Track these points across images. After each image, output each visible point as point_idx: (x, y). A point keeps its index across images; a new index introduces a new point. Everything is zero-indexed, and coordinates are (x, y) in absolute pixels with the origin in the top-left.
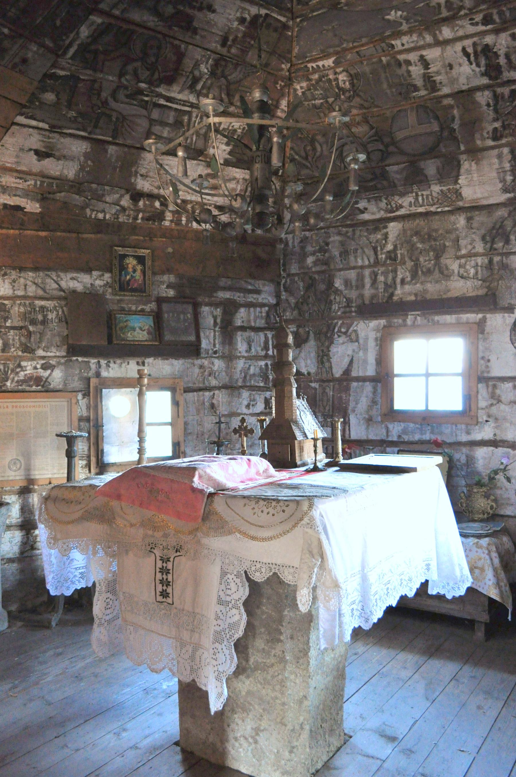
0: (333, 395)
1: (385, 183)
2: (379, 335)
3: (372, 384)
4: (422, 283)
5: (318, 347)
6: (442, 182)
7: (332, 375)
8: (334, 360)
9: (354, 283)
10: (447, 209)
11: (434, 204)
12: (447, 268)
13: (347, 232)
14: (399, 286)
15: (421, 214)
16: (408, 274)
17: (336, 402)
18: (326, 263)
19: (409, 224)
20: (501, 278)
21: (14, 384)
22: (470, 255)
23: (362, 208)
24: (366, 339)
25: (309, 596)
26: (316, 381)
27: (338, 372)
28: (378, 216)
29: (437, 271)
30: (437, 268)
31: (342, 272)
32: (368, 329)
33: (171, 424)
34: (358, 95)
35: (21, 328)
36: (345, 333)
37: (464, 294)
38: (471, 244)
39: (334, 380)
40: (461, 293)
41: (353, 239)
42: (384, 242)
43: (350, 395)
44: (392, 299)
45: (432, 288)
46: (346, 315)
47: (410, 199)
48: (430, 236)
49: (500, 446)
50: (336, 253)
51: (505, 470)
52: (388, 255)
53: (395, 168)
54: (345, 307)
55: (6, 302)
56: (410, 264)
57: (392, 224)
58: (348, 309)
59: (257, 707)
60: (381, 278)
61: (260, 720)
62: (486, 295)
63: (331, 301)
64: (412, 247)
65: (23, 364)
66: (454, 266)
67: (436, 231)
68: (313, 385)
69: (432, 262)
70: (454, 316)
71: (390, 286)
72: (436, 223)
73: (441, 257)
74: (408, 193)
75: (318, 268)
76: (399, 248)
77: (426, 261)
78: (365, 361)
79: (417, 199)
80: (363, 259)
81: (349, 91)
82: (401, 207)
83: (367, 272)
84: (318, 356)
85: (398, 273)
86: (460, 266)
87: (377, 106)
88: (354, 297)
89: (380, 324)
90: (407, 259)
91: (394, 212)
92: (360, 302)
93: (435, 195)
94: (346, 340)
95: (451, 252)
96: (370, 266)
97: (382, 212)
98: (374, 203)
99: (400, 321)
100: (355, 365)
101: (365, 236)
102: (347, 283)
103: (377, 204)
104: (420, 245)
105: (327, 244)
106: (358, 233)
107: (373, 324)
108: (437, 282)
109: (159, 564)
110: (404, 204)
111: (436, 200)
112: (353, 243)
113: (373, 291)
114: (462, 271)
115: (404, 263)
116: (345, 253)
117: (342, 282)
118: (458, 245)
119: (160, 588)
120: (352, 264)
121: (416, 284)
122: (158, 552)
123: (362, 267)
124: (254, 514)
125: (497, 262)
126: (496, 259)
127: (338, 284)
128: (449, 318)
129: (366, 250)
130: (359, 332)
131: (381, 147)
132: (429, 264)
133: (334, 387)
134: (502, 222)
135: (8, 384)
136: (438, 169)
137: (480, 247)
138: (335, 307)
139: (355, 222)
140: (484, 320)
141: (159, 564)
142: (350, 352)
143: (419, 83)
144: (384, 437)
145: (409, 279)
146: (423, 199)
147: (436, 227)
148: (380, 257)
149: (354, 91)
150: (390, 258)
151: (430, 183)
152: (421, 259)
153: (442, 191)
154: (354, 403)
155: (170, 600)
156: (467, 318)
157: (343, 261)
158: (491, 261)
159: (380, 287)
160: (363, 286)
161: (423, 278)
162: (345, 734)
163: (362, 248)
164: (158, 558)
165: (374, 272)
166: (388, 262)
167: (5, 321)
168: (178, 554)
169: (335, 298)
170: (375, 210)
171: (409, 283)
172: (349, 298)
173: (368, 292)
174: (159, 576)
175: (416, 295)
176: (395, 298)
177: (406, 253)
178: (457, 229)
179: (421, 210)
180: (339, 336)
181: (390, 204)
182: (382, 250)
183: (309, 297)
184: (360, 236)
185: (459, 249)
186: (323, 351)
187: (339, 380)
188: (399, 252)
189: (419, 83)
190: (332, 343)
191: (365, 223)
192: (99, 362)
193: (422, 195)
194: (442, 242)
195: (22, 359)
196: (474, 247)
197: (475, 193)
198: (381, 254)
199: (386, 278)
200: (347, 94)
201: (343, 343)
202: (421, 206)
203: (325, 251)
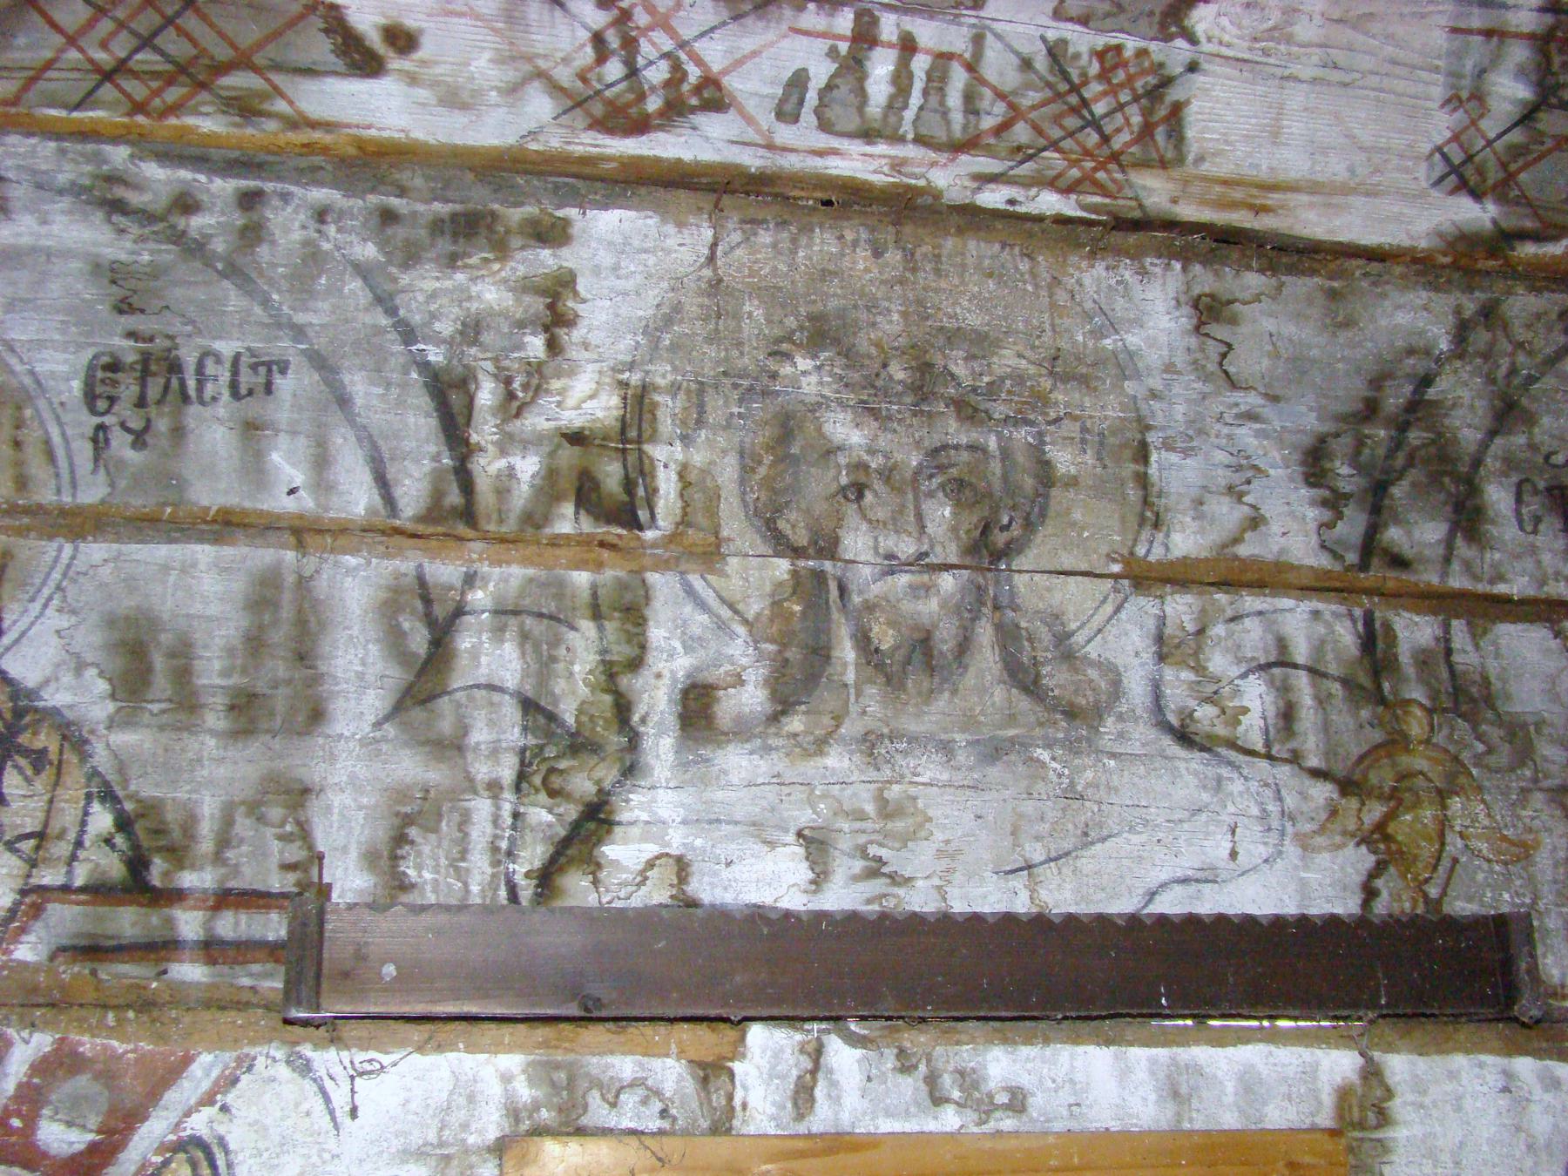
12: (1068, 655)
16: (739, 650)
28: (491, 131)
29: (987, 657)
30: (985, 633)
42: (536, 345)
52: (569, 456)
56: (753, 574)
60: (490, 658)
66: (1122, 638)
69: (947, 582)
71: (580, 745)
76: (666, 425)
77: (891, 565)
79: (853, 66)
85: (657, 634)
90: (734, 525)
96: (384, 531)
97: (540, 106)
101: (362, 270)
110: (734, 83)
114: (1178, 685)
129: (359, 385)
132: (916, 591)
148: (487, 467)
150: (586, 494)
152: (857, 543)
159: (480, 735)
161: (871, 706)
165: (424, 591)
166: (567, 520)
177: (727, 473)
182: (512, 406)
188: (665, 456)
191: (371, 163)
193: (908, 46)
199: (544, 662)
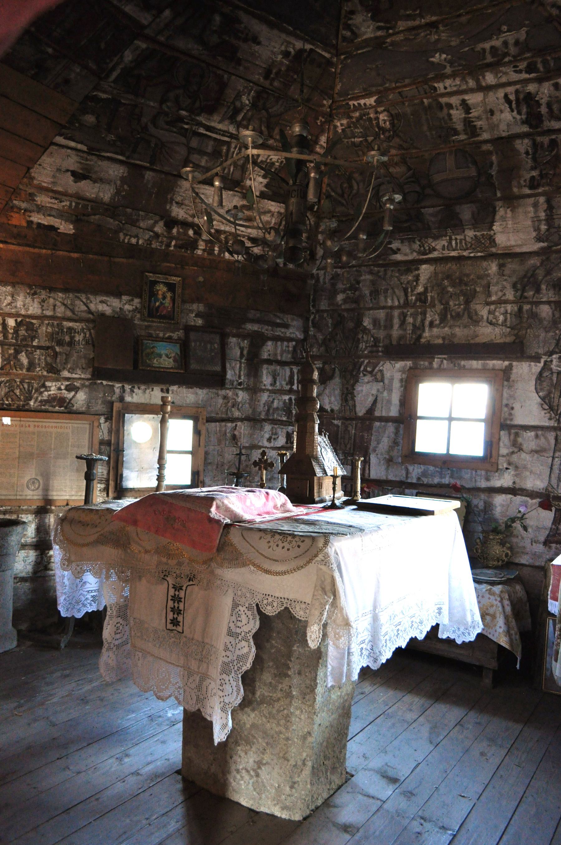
0: (355, 433)
1: (419, 224)
2: (404, 376)
3: (394, 425)
4: (450, 327)
5: (343, 385)
6: (476, 228)
7: (356, 414)
8: (358, 398)
9: (382, 323)
10: (479, 254)
11: (467, 249)
12: (476, 314)
13: (379, 272)
14: (427, 329)
15: (453, 258)
16: (437, 317)
17: (358, 441)
18: (356, 301)
19: (441, 268)
20: (530, 327)
21: (37, 404)
22: (500, 302)
23: (395, 248)
24: (392, 379)
25: (319, 633)
26: (338, 419)
27: (361, 411)
28: (410, 258)
29: (466, 315)
30: (466, 313)
31: (371, 312)
32: (393, 370)
33: (191, 453)
34: (398, 136)
35: (48, 348)
36: (371, 373)
37: (492, 340)
38: (501, 291)
39: (357, 418)
40: (489, 339)
41: (384, 279)
42: (415, 283)
43: (372, 435)
44: (419, 341)
45: (460, 333)
46: (373, 354)
47: (444, 242)
48: (461, 281)
49: (519, 495)
50: (367, 292)
51: (522, 518)
53: (431, 210)
54: (372, 346)
55: (34, 321)
56: (439, 307)
57: (424, 266)
58: (375, 349)
59: (260, 740)
60: (410, 320)
61: (263, 754)
62: (514, 342)
63: (359, 339)
64: (443, 291)
65: (48, 384)
66: (484, 312)
67: (468, 275)
68: (336, 422)
69: (462, 307)
70: (480, 362)
71: (419, 328)
72: (468, 268)
73: (471, 302)
74: (442, 236)
75: (347, 306)
77: (455, 305)
78: (389, 402)
79: (450, 243)
80: (393, 300)
81: (389, 131)
82: (434, 249)
83: (396, 313)
84: (343, 394)
86: (490, 312)
87: (416, 148)
88: (382, 337)
89: (406, 365)
91: (427, 254)
92: (387, 342)
93: (468, 239)
94: (371, 379)
95: (481, 298)
96: (399, 307)
97: (415, 254)
98: (407, 244)
99: (426, 363)
100: (379, 405)
101: (397, 277)
102: (376, 322)
103: (410, 246)
104: (450, 289)
105: (358, 282)
106: (389, 273)
107: (399, 365)
108: (465, 327)
109: (172, 592)
110: (437, 247)
111: (469, 245)
112: (384, 283)
113: (401, 332)
114: (491, 317)
115: (434, 306)
116: (375, 293)
117: (371, 321)
118: (489, 291)
119: (171, 616)
120: (382, 304)
121: (444, 327)
122: (171, 580)
123: (392, 308)
124: (269, 547)
125: (527, 311)
126: (526, 307)
127: (367, 323)
128: (475, 364)
129: (396, 290)
130: (385, 372)
131: (418, 189)
132: (458, 308)
133: (356, 426)
134: (534, 271)
135: (32, 403)
136: (473, 214)
137: (510, 295)
138: (362, 345)
139: (387, 262)
140: (510, 367)
141: (172, 592)
142: (374, 392)
143: (460, 127)
144: (403, 479)
145: (438, 322)
146: (456, 243)
147: (468, 272)
148: (410, 298)
149: (394, 132)
150: (420, 300)
151: (465, 227)
152: (451, 303)
153: (475, 236)
154: (376, 443)
155: (180, 629)
156: (494, 365)
157: (373, 300)
158: (520, 309)
160: (392, 327)
161: (451, 322)
162: (347, 773)
163: (393, 289)
164: (171, 586)
165: (403, 313)
167: (32, 340)
168: (191, 583)
169: (363, 337)
170: (408, 251)
171: (438, 326)
172: (377, 338)
173: (396, 332)
174: (171, 604)
175: (444, 338)
176: (423, 340)
177: (436, 296)
178: (488, 275)
179: (453, 254)
180: (365, 375)
181: (423, 246)
182: (412, 291)
183: (337, 334)
184: (392, 276)
185: (489, 295)
186: (347, 389)
187: (362, 419)
188: (429, 295)
189: (460, 127)
190: (357, 381)
191: (398, 263)
192: (123, 386)
193: (456, 239)
194: (473, 287)
195: (47, 379)
196: (504, 295)
197: (509, 240)
198: (411, 296)
199: (415, 320)
200: (387, 134)
201: (368, 383)
202: (454, 250)
203: (356, 289)
